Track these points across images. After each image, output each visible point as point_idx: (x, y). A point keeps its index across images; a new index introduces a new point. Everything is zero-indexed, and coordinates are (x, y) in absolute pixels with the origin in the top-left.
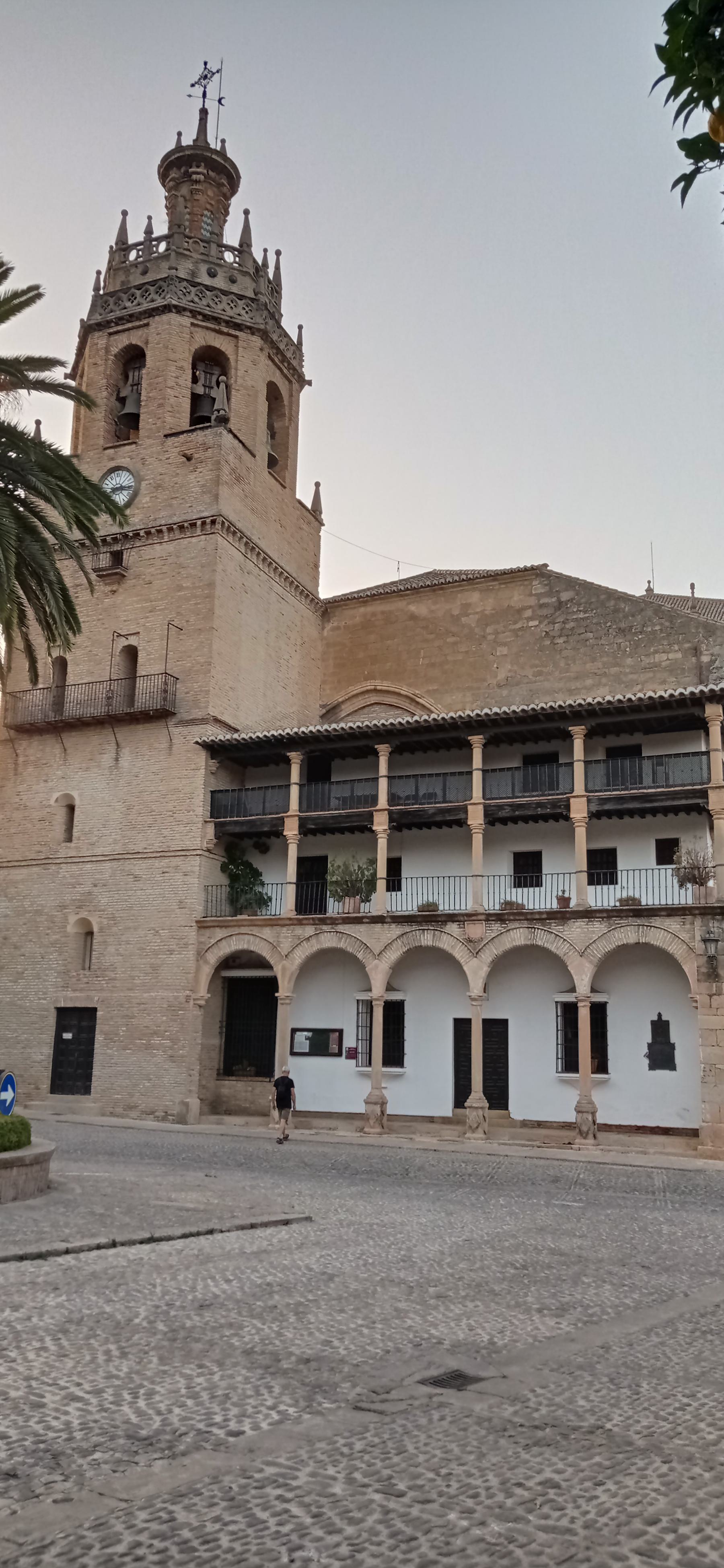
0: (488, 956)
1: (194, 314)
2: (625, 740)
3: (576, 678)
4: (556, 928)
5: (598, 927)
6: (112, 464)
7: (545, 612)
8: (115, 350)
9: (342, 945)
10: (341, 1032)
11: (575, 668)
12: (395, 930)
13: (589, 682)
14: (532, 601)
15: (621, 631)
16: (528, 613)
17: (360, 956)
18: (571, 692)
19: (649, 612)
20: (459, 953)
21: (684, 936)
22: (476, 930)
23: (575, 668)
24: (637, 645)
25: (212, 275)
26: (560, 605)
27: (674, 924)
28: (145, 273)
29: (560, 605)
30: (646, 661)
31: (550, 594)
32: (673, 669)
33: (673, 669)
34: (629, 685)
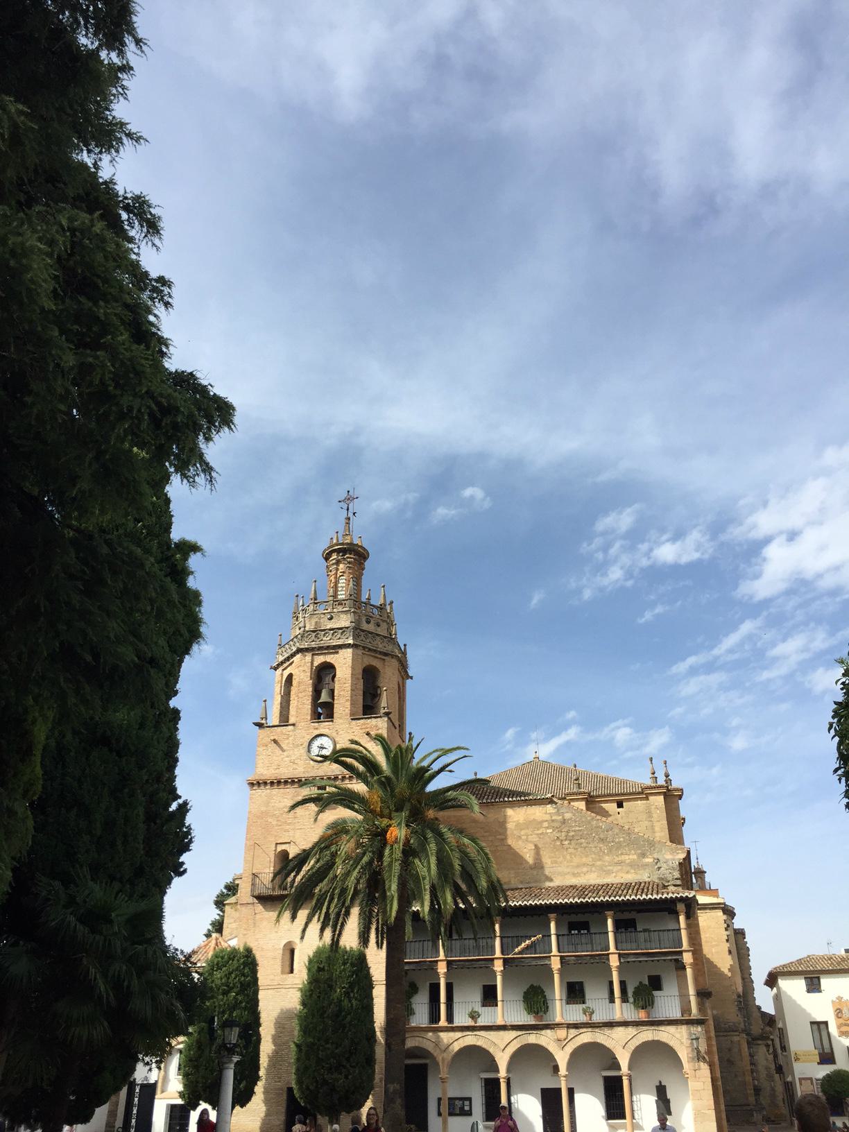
0: (569, 1049)
1: (364, 648)
2: (627, 916)
3: (578, 866)
4: (607, 1031)
5: (631, 1031)
6: (317, 732)
7: (556, 824)
8: (316, 664)
9: (479, 1043)
10: (470, 1099)
11: (576, 860)
12: (514, 1034)
13: (585, 869)
14: (547, 817)
15: (602, 840)
16: (546, 824)
17: (491, 1050)
18: (574, 875)
19: (616, 831)
20: (552, 1048)
21: (678, 1036)
22: (562, 1033)
23: (576, 860)
24: (610, 850)
25: (368, 622)
26: (564, 822)
27: (671, 1029)
28: (331, 619)
29: (564, 822)
30: (617, 859)
31: (558, 813)
32: (633, 865)
33: (633, 865)
34: (608, 873)
